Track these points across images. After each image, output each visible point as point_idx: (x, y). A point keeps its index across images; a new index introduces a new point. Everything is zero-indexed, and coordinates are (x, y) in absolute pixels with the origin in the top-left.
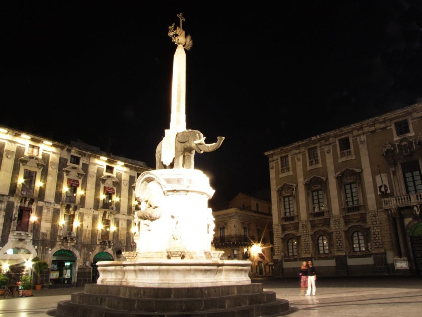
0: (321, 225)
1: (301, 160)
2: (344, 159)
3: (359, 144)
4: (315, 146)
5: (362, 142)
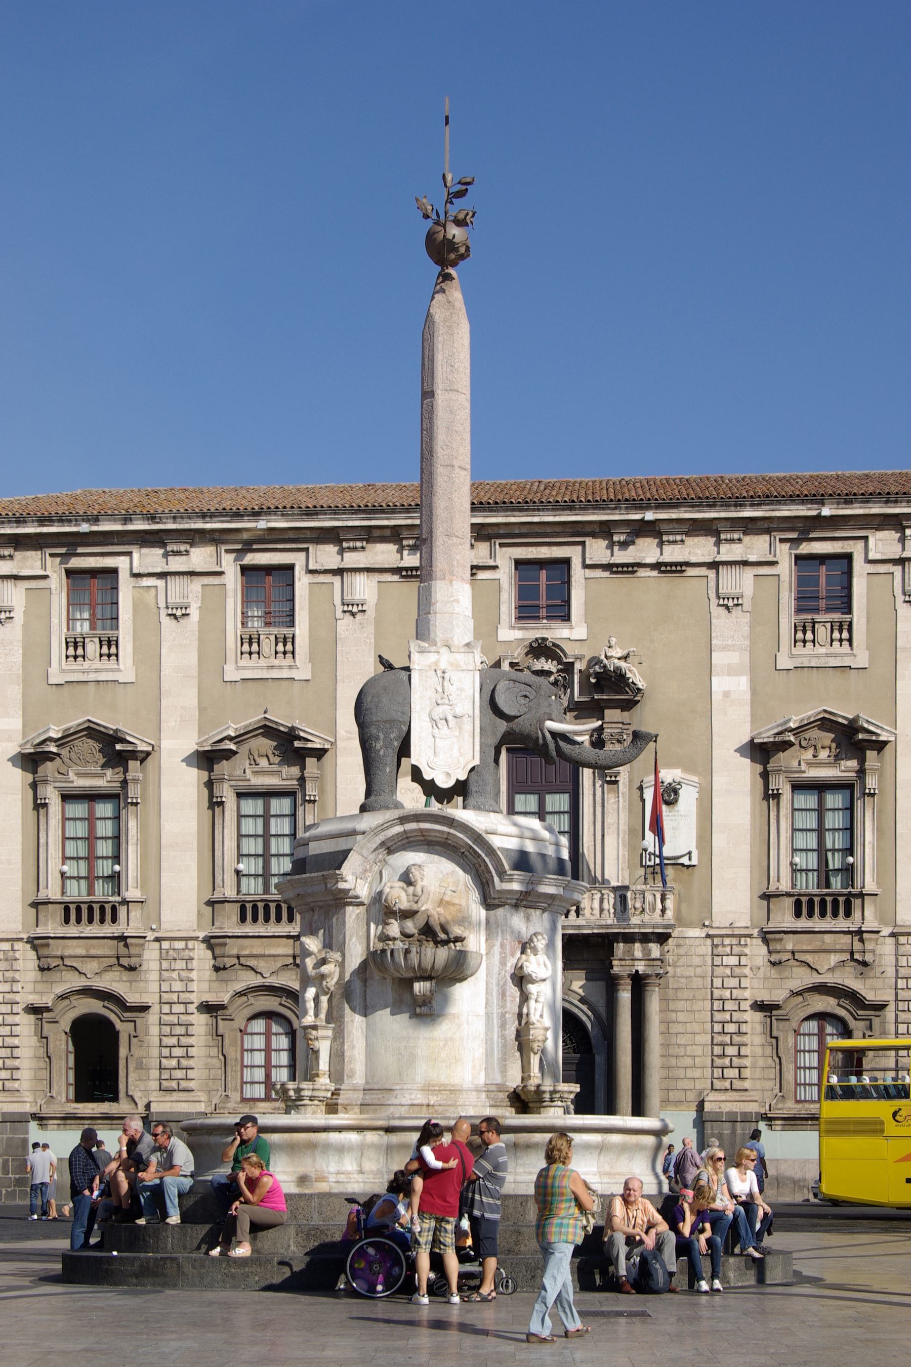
0: (91, 967)
1: (18, 615)
2: (253, 668)
3: (339, 614)
4: (109, 562)
5: (353, 609)
